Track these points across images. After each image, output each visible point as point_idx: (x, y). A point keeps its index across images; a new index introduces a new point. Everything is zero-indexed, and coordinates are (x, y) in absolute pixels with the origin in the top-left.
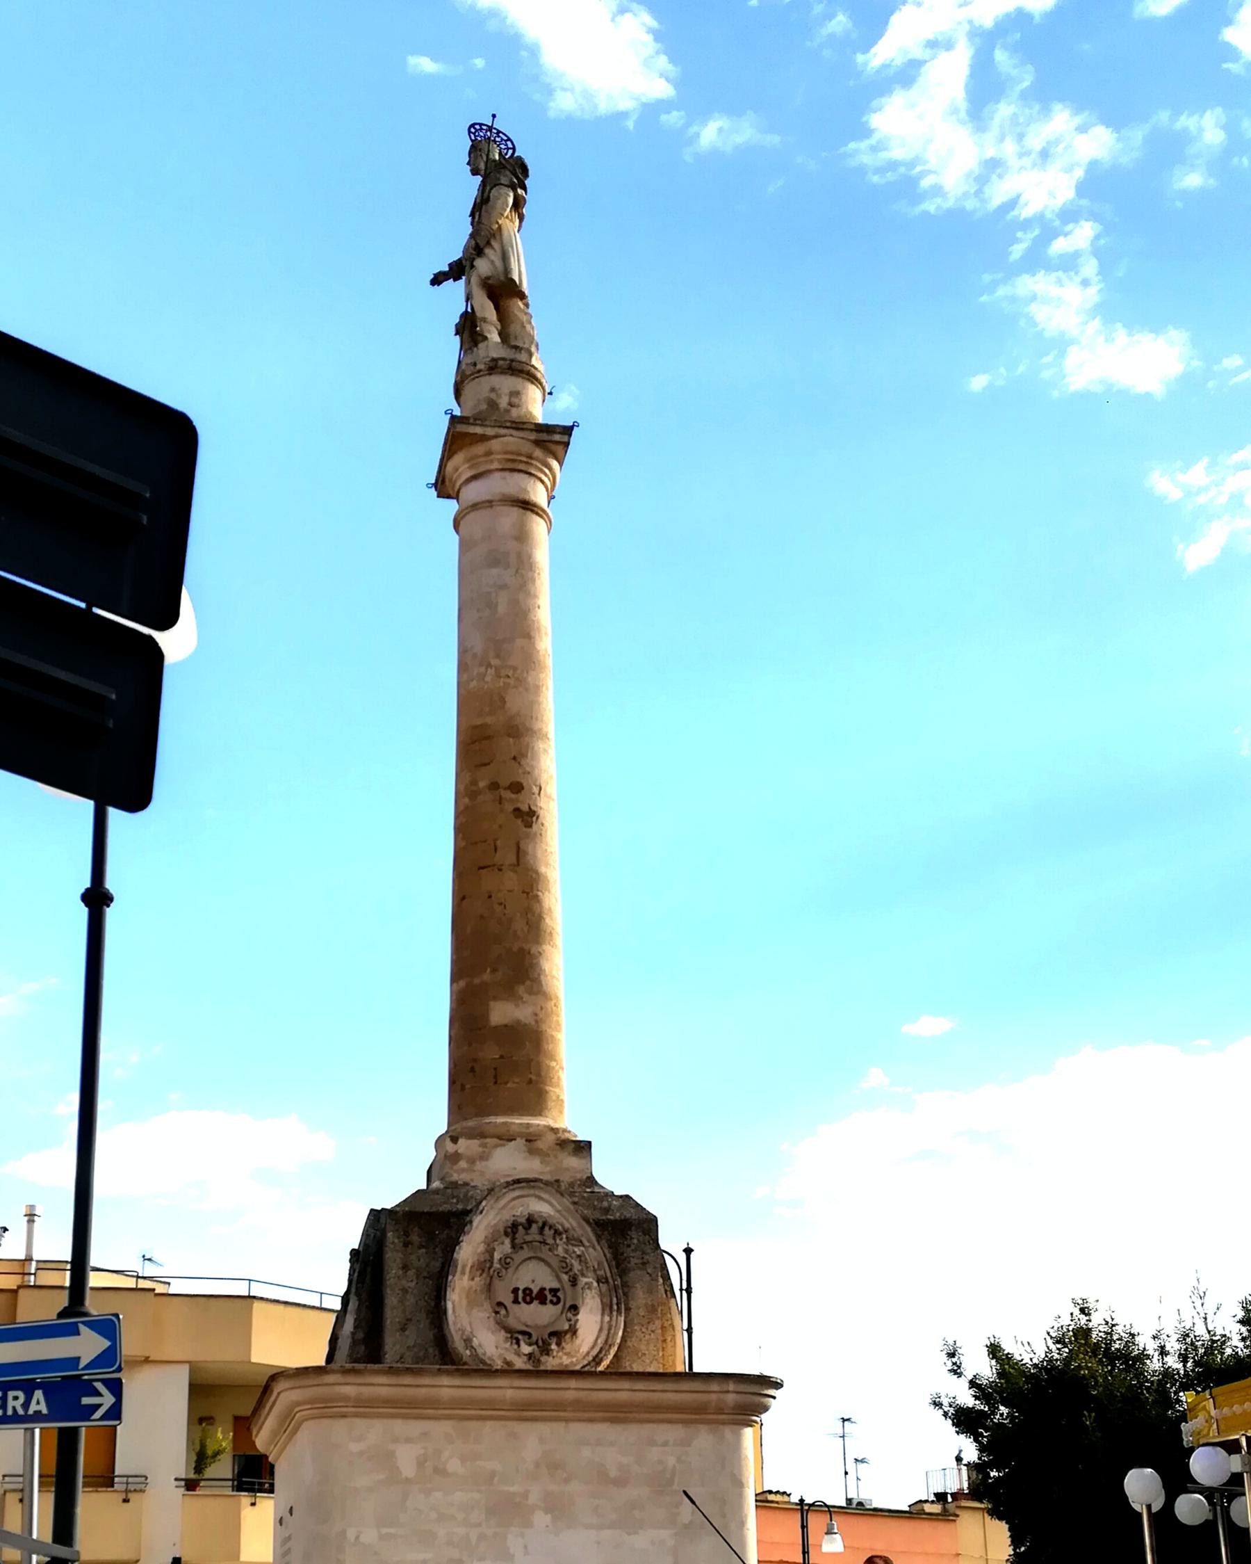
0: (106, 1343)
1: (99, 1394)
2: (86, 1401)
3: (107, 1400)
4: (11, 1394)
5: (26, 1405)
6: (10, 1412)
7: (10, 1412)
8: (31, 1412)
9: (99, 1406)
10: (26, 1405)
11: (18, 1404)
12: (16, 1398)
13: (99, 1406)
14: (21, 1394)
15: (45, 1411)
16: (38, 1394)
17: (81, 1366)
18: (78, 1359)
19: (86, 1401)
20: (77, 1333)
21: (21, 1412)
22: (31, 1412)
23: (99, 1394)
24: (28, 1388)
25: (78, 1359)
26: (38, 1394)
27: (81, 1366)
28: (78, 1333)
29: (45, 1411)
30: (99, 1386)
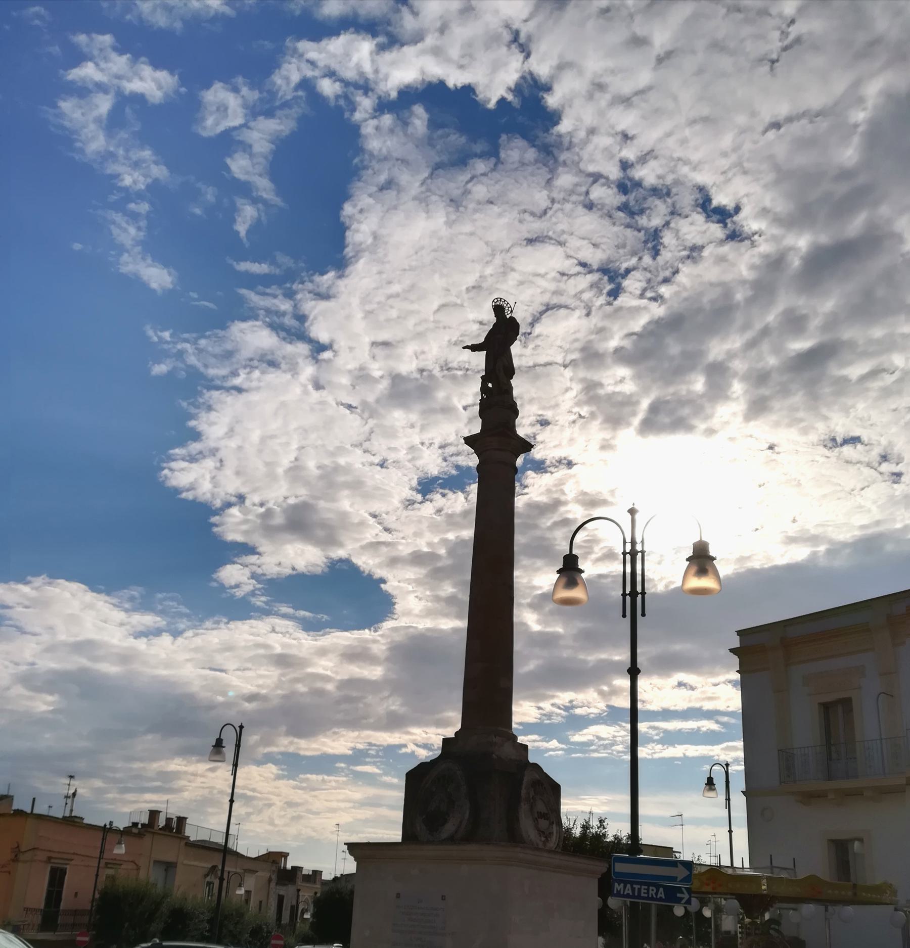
0: (689, 873)
1: (683, 893)
2: (678, 895)
3: (686, 896)
4: (651, 888)
5: (656, 894)
6: (650, 896)
7: (650, 896)
8: (658, 897)
9: (684, 898)
10: (656, 894)
11: (654, 893)
12: (653, 890)
13: (684, 898)
14: (654, 888)
15: (664, 897)
16: (661, 890)
17: (678, 880)
18: (677, 877)
19: (678, 895)
20: (677, 867)
21: (655, 896)
22: (658, 897)
23: (683, 893)
24: (658, 887)
25: (677, 877)
26: (661, 890)
27: (678, 880)
28: (677, 867)
29: (664, 897)
30: (683, 889)
